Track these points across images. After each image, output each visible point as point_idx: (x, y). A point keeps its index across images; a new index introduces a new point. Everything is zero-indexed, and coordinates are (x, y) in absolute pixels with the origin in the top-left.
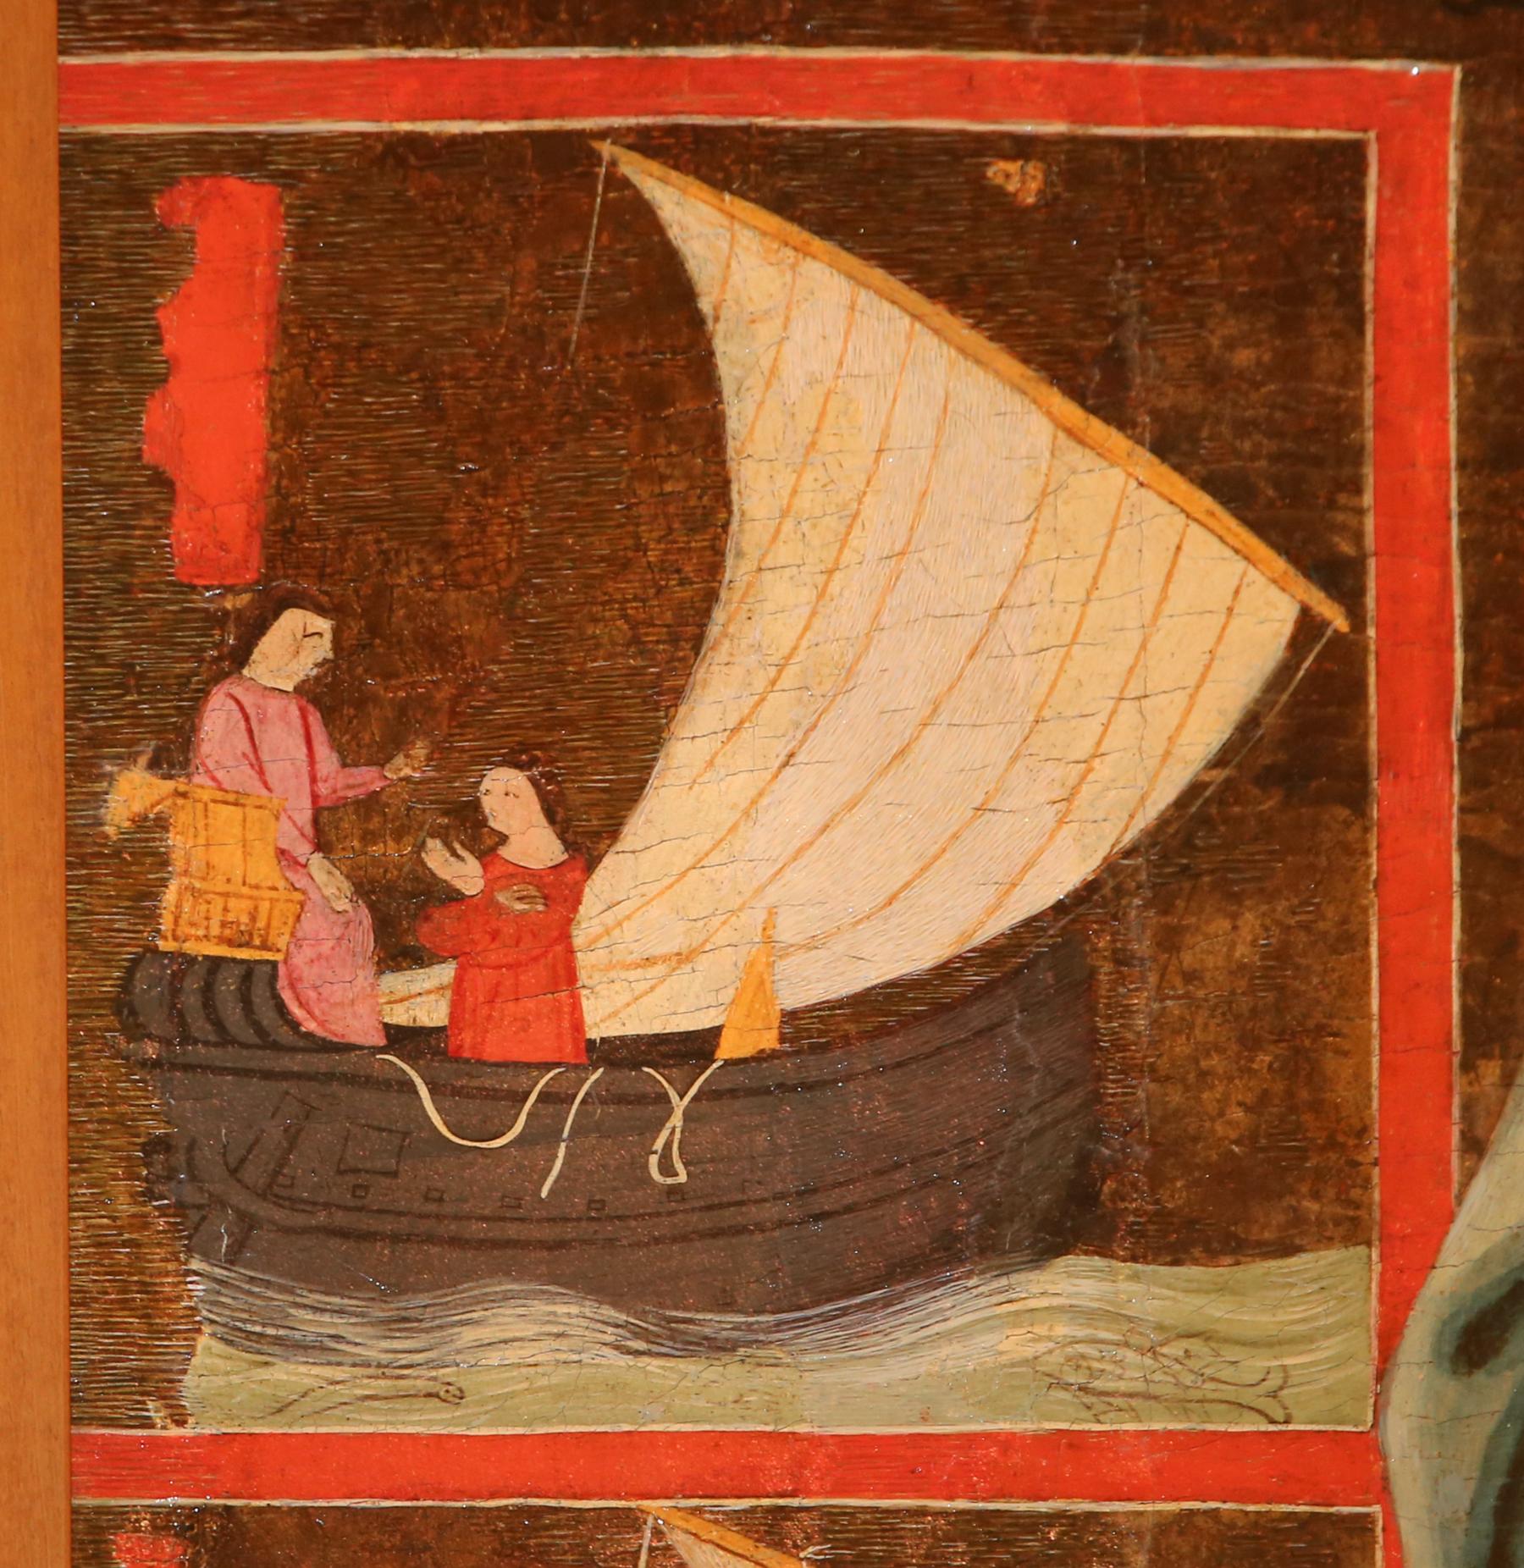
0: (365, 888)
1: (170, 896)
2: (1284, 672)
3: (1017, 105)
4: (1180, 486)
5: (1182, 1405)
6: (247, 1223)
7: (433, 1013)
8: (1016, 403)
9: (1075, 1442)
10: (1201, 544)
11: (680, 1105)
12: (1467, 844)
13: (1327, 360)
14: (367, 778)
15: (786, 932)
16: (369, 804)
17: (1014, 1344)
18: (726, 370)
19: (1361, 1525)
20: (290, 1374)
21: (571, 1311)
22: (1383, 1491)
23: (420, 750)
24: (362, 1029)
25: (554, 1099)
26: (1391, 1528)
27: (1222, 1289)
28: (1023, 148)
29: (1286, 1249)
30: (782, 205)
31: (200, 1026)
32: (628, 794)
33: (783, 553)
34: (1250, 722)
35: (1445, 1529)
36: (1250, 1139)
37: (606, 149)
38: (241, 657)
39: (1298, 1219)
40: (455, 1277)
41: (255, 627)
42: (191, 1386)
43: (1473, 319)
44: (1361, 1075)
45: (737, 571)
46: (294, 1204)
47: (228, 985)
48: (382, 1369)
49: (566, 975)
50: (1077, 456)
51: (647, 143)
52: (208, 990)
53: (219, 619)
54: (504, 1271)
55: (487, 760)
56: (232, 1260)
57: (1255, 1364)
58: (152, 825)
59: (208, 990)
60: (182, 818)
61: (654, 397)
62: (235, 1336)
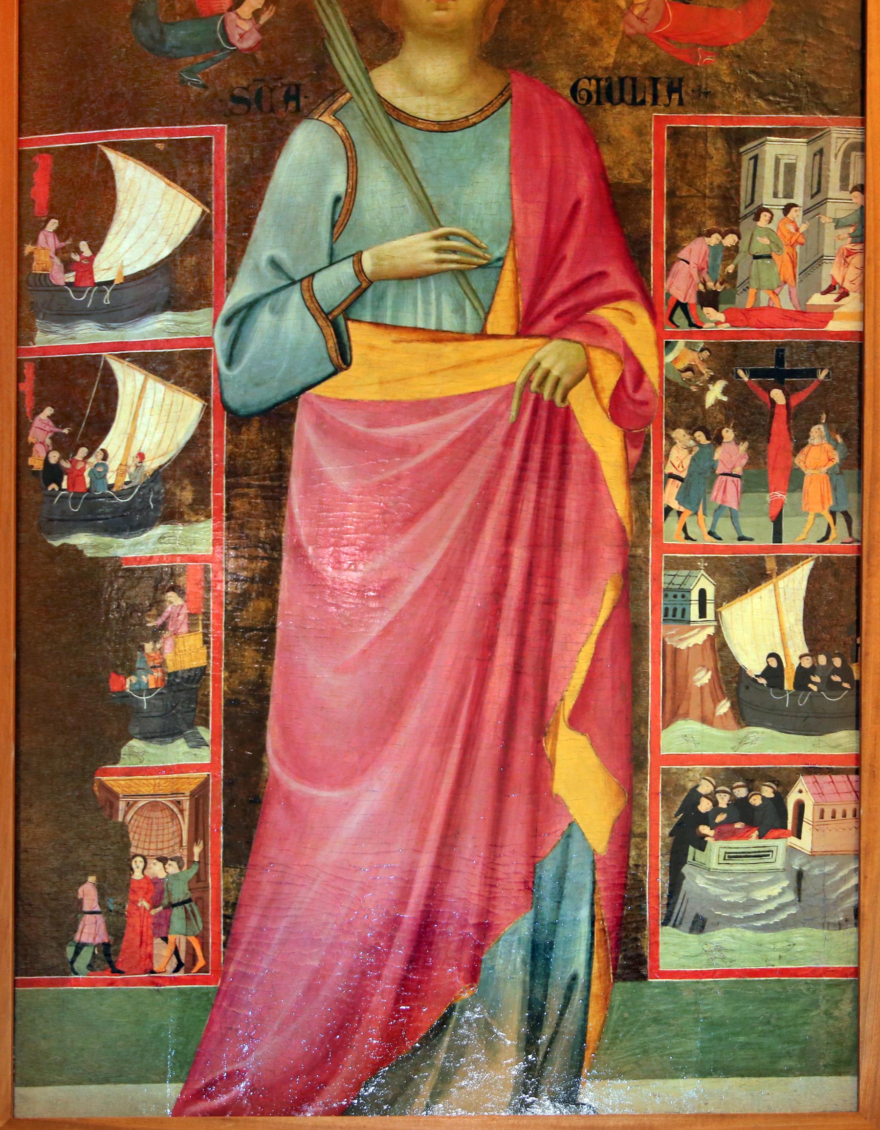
0: (62, 261)
1: (34, 264)
2: (200, 219)
3: (160, 135)
4: (185, 192)
5: (183, 334)
6: (45, 314)
7: (72, 280)
8: (159, 180)
9: (167, 340)
10: (188, 201)
11: (109, 291)
12: (228, 245)
13: (207, 172)
14: (63, 244)
15: (125, 264)
16: (63, 248)
17: (158, 325)
18: (117, 178)
19: (210, 351)
20: (51, 336)
21: (92, 324)
22: (213, 345)
23: (71, 239)
24: (62, 283)
25: (90, 292)
27: (190, 315)
28: (161, 141)
29: (199, 309)
30: (124, 152)
31: (38, 283)
32: (101, 244)
33: (125, 206)
34: (195, 227)
35: (223, 351)
36: (194, 292)
37: (99, 146)
38: (45, 226)
39: (201, 304)
40: (73, 321)
41: (47, 222)
42: (37, 339)
43: (229, 163)
44: (211, 282)
45: (118, 209)
46: (51, 310)
47: (42, 278)
48: (65, 335)
49: (91, 272)
50: (169, 188)
51: (105, 144)
52: (39, 279)
53: (42, 221)
54: (82, 319)
55: (80, 240)
56: (43, 319)
57: (196, 326)
58: (31, 254)
59: (39, 279)
60: (36, 252)
61: (106, 182)
62: (43, 331)
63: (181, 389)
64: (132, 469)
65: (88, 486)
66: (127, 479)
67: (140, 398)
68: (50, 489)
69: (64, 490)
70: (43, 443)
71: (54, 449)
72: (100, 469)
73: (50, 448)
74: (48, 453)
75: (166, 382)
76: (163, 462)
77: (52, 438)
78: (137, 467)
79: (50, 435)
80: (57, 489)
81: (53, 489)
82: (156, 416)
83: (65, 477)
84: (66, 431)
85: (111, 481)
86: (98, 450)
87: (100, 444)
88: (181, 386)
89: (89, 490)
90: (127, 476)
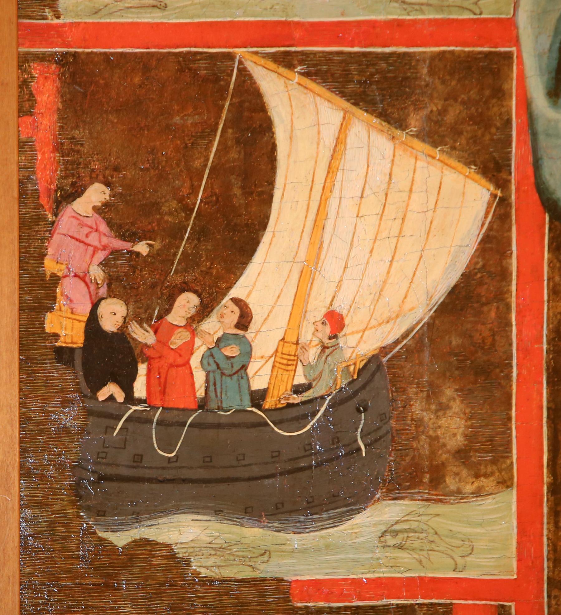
19: (508, 56)
22: (517, 42)
26: (520, 57)
35: (540, 56)
63: (437, 152)
64: (313, 354)
65: (200, 393)
66: (300, 379)
67: (331, 170)
68: (103, 395)
69: (140, 401)
70: (83, 277)
71: (111, 294)
72: (232, 351)
73: (103, 291)
74: (95, 306)
75: (398, 132)
76: (390, 340)
77: (104, 264)
78: (324, 348)
79: (101, 256)
80: (120, 397)
81: (111, 398)
82: (375, 220)
83: (142, 369)
84: (142, 248)
85: (258, 384)
86: (226, 300)
87: (229, 288)
88: (435, 145)
89: (203, 404)
90: (300, 368)
